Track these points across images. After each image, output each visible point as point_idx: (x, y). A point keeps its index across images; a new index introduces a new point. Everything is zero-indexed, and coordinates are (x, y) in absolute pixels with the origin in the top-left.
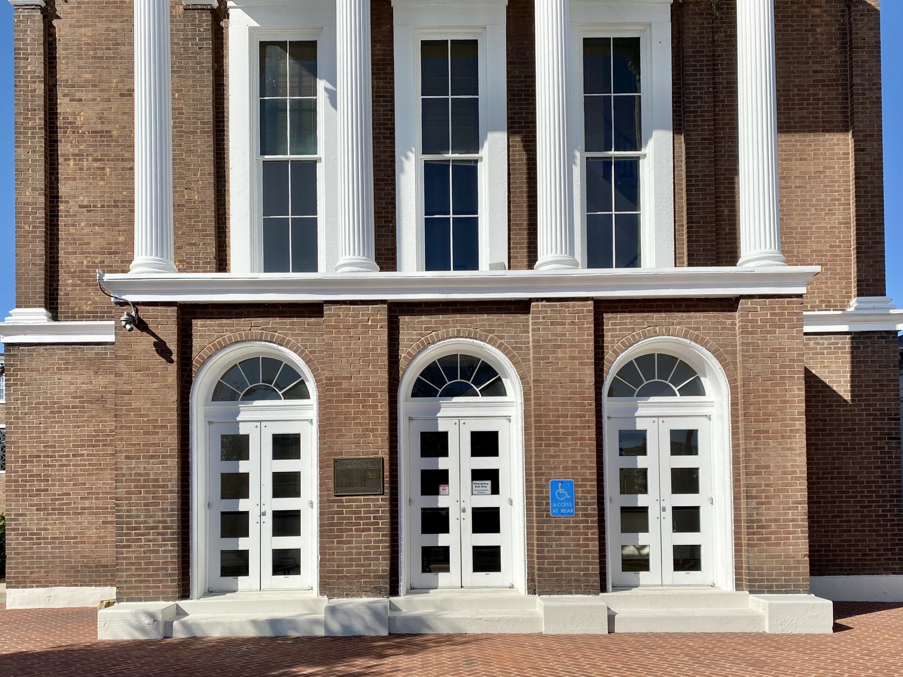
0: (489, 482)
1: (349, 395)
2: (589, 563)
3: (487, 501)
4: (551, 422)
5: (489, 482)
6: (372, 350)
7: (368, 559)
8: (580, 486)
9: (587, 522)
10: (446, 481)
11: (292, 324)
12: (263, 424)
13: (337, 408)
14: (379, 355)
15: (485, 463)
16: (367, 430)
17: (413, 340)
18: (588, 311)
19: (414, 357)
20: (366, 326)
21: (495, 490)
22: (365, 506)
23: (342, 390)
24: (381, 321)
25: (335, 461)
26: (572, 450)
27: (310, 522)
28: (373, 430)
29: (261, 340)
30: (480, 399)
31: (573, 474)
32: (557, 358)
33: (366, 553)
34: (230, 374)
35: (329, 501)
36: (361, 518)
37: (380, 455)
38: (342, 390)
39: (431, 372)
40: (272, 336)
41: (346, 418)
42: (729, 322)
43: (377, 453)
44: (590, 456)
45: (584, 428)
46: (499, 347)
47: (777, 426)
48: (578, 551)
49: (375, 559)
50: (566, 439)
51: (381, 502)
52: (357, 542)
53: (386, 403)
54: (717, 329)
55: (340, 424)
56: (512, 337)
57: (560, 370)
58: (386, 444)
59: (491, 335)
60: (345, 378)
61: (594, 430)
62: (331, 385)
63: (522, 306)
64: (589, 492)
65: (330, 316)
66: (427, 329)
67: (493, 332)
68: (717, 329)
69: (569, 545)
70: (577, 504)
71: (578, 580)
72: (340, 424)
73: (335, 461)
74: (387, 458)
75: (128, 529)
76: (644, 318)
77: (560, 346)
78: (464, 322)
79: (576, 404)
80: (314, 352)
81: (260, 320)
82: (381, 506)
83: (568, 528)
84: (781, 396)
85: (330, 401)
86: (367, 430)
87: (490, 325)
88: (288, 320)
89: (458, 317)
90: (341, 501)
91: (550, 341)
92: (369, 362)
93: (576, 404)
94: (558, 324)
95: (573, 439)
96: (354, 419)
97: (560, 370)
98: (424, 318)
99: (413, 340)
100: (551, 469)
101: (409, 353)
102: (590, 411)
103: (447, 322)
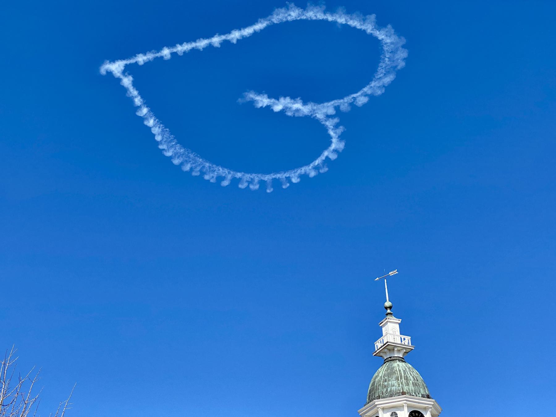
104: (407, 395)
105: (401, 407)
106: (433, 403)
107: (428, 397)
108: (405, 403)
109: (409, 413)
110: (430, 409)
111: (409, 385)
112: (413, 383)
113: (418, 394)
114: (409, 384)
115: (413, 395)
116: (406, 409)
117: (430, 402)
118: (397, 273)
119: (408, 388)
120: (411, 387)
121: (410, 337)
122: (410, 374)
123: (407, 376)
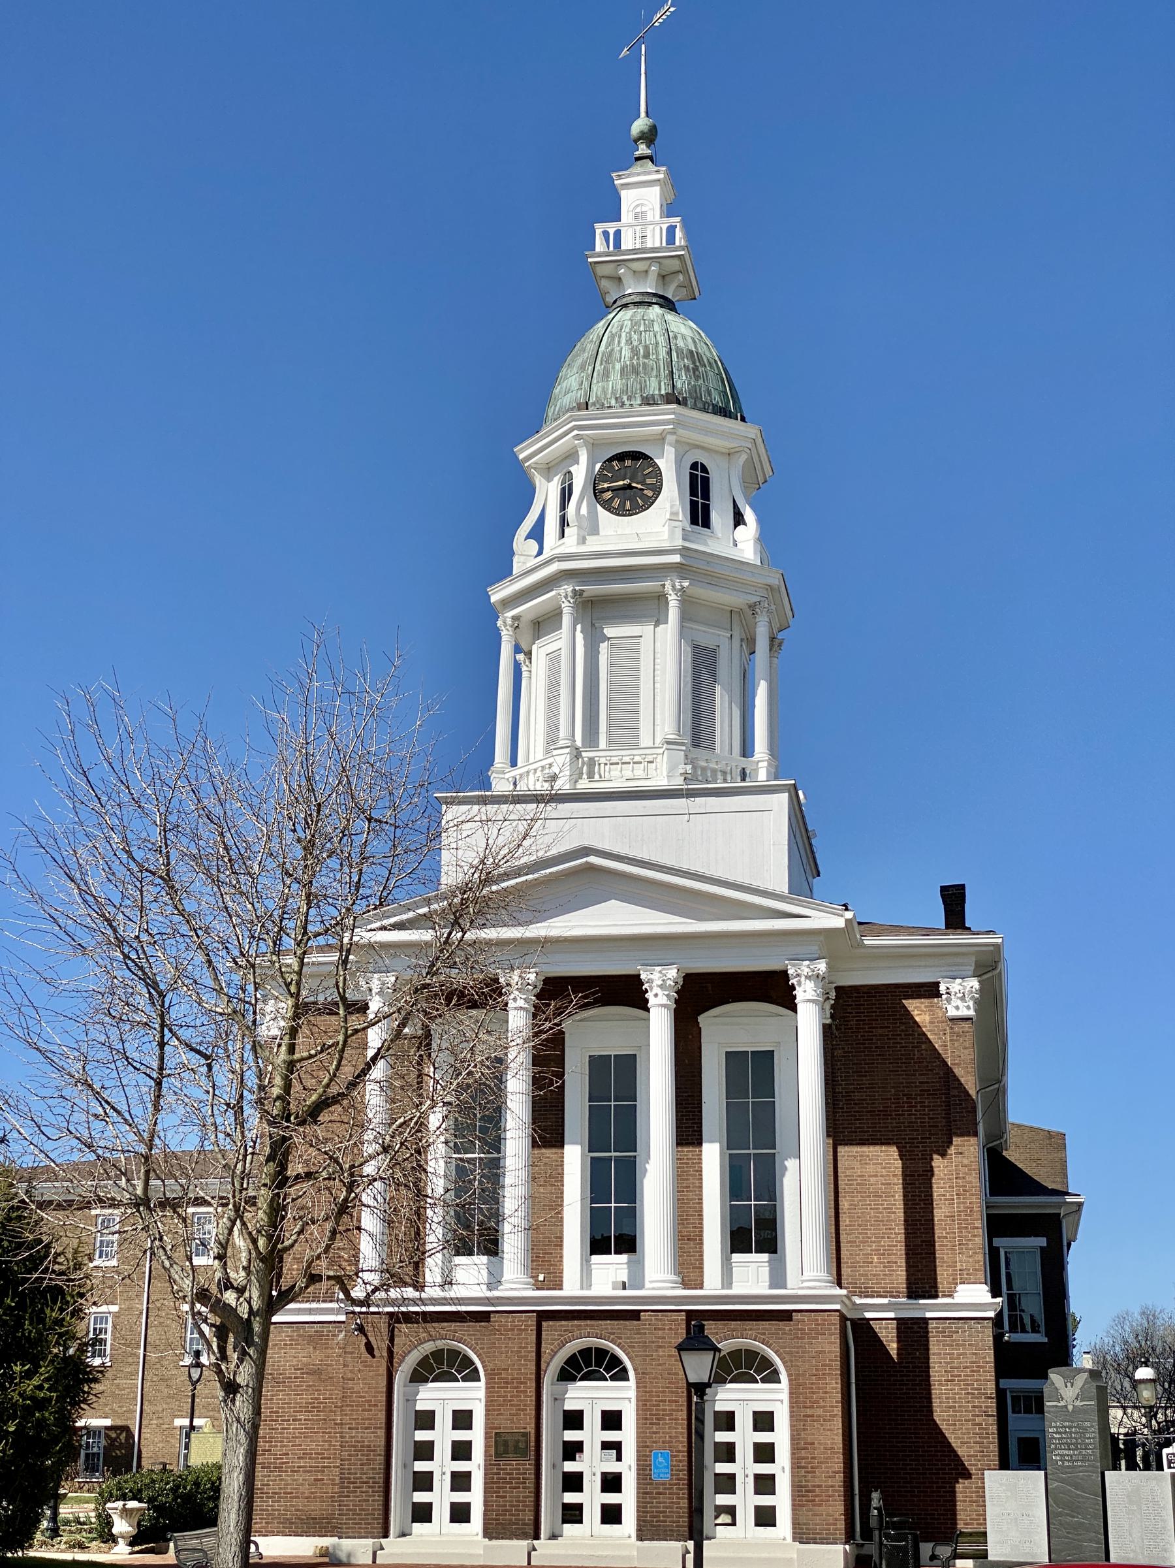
0: (615, 1451)
1: (507, 1383)
2: (680, 1517)
3: (613, 1467)
4: (654, 1406)
5: (615, 1451)
6: (524, 1348)
7: (518, 1510)
8: (675, 1456)
9: (679, 1484)
10: (581, 1451)
11: (468, 1326)
12: (446, 1402)
13: (498, 1392)
14: (529, 1352)
15: (612, 1436)
16: (519, 1410)
17: (555, 1340)
18: (682, 1320)
19: (556, 1353)
20: (520, 1330)
21: (619, 1459)
22: (516, 1469)
23: (502, 1378)
24: (532, 1325)
25: (496, 1434)
26: (669, 1428)
27: (478, 1482)
28: (523, 1410)
29: (446, 1339)
30: (610, 1383)
31: (670, 1447)
32: (659, 1356)
33: (516, 1506)
34: (424, 1363)
35: (491, 1465)
36: (513, 1478)
37: (528, 1430)
38: (502, 1378)
39: (572, 1361)
40: (454, 1336)
41: (504, 1401)
42: (787, 1328)
43: (525, 1428)
44: (682, 1433)
45: (678, 1411)
46: (618, 1346)
47: (820, 1411)
48: (672, 1508)
49: (522, 1511)
50: (665, 1419)
51: (529, 1466)
52: (510, 1497)
53: (533, 1389)
54: (778, 1334)
55: (499, 1405)
56: (628, 1338)
57: (660, 1365)
58: (533, 1421)
59: (612, 1336)
60: (504, 1369)
61: (685, 1412)
62: (494, 1374)
63: (635, 1315)
64: (680, 1461)
65: (495, 1322)
66: (565, 1331)
67: (614, 1333)
68: (778, 1334)
69: (665, 1502)
70: (672, 1470)
71: (672, 1530)
72: (499, 1405)
73: (496, 1434)
74: (533, 1431)
75: (348, 1483)
76: (725, 1325)
77: (660, 1347)
78: (593, 1325)
79: (672, 1392)
80: (483, 1348)
81: (446, 1324)
82: (527, 1469)
83: (665, 1489)
84: (822, 1388)
85: (494, 1387)
86: (519, 1410)
87: (612, 1329)
88: (465, 1324)
89: (589, 1322)
90: (499, 1465)
91: (653, 1342)
92: (522, 1357)
93: (672, 1392)
94: (659, 1329)
95: (670, 1419)
96: (510, 1401)
97: (660, 1365)
98: (563, 1323)
99: (555, 1340)
100: (654, 1442)
101: (552, 1350)
102: (681, 1397)
103: (580, 1325)
104: (593, 411)
105: (571, 456)
106: (673, 416)
107: (672, 398)
108: (577, 437)
109: (598, 466)
110: (670, 438)
111: (608, 377)
112: (622, 370)
113: (629, 398)
114: (608, 373)
115: (610, 407)
116: (583, 457)
117: (668, 413)
118: (672, 9)
119: (603, 388)
120: (615, 381)
121: (678, 219)
122: (629, 341)
123: (613, 350)
